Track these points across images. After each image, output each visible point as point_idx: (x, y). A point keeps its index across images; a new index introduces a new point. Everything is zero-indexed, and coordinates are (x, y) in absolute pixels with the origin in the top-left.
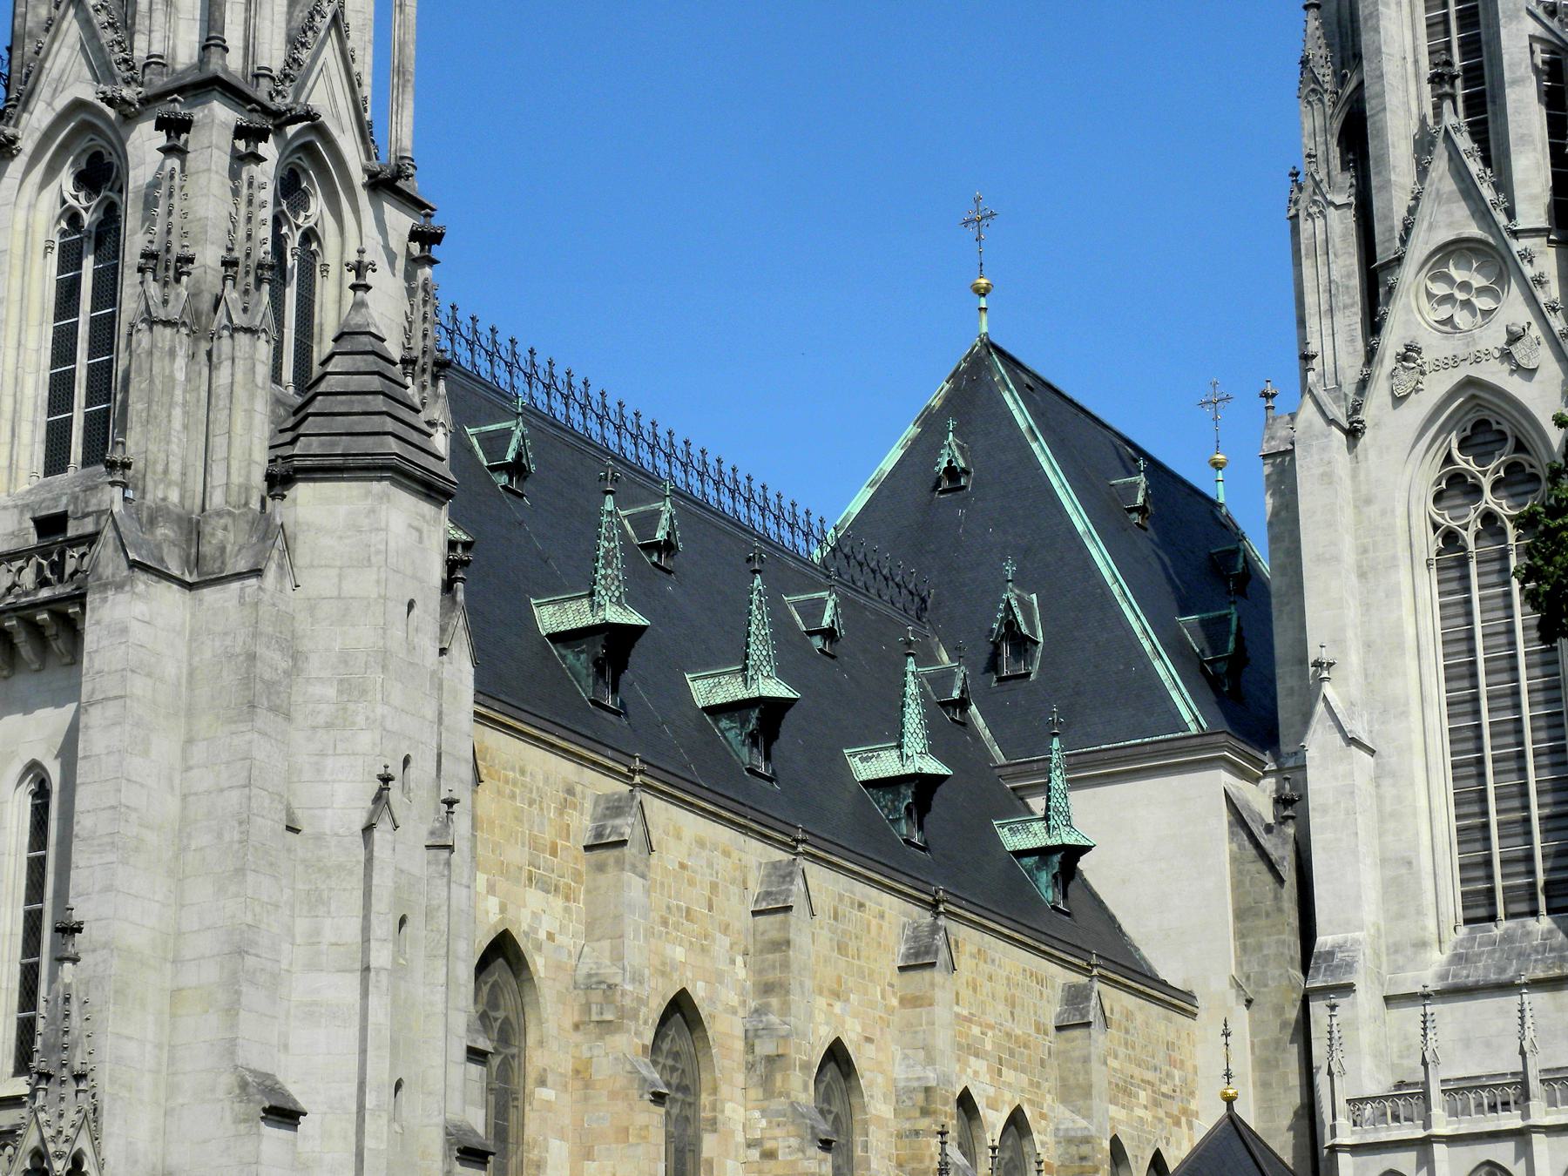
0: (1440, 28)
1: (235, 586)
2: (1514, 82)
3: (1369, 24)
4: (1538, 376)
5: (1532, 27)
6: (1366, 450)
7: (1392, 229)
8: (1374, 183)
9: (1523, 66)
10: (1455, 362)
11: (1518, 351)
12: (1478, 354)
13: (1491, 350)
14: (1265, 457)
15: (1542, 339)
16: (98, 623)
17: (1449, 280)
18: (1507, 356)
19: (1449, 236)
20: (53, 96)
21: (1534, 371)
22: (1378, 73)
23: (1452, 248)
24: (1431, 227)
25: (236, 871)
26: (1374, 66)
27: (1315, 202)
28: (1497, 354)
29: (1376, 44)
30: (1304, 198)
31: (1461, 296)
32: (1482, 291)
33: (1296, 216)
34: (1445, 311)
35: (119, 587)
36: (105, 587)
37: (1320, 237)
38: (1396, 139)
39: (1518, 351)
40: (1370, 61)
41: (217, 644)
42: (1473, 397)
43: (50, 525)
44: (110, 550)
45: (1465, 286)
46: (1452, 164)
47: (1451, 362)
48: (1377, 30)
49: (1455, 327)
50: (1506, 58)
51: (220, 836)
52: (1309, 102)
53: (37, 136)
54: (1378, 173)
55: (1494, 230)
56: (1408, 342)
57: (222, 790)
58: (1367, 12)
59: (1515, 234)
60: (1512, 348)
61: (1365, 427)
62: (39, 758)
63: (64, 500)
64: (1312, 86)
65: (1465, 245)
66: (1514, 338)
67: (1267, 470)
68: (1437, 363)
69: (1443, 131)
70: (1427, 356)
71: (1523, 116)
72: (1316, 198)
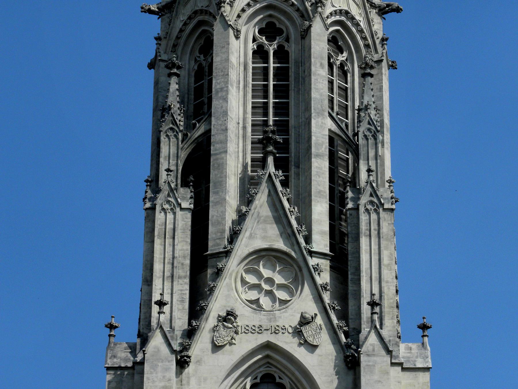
0: (260, 111)
2: (318, 156)
3: (220, 95)
4: (318, 351)
5: (330, 124)
6: (189, 378)
7: (224, 231)
8: (211, 199)
9: (324, 146)
10: (260, 330)
11: (307, 331)
12: (277, 328)
13: (287, 326)
14: (108, 369)
15: (323, 327)
17: (259, 275)
19: (265, 245)
21: (316, 347)
22: (223, 127)
23: (263, 253)
24: (251, 237)
26: (220, 122)
27: (168, 202)
28: (290, 330)
29: (224, 108)
30: (161, 199)
31: (266, 287)
32: (281, 287)
33: (153, 208)
34: (253, 295)
37: (170, 226)
38: (230, 173)
39: (307, 331)
40: (218, 119)
42: (268, 356)
45: (270, 281)
46: (270, 198)
47: (257, 330)
48: (226, 100)
49: (260, 306)
50: (313, 138)
52: (167, 136)
54: (217, 193)
55: (296, 247)
56: (229, 309)
58: (218, 87)
59: (312, 253)
60: (303, 328)
61: (190, 362)
64: (171, 126)
65: (279, 255)
66: (305, 321)
67: (109, 377)
68: (247, 328)
69: (267, 175)
70: (240, 322)
71: (321, 178)
72: (170, 199)
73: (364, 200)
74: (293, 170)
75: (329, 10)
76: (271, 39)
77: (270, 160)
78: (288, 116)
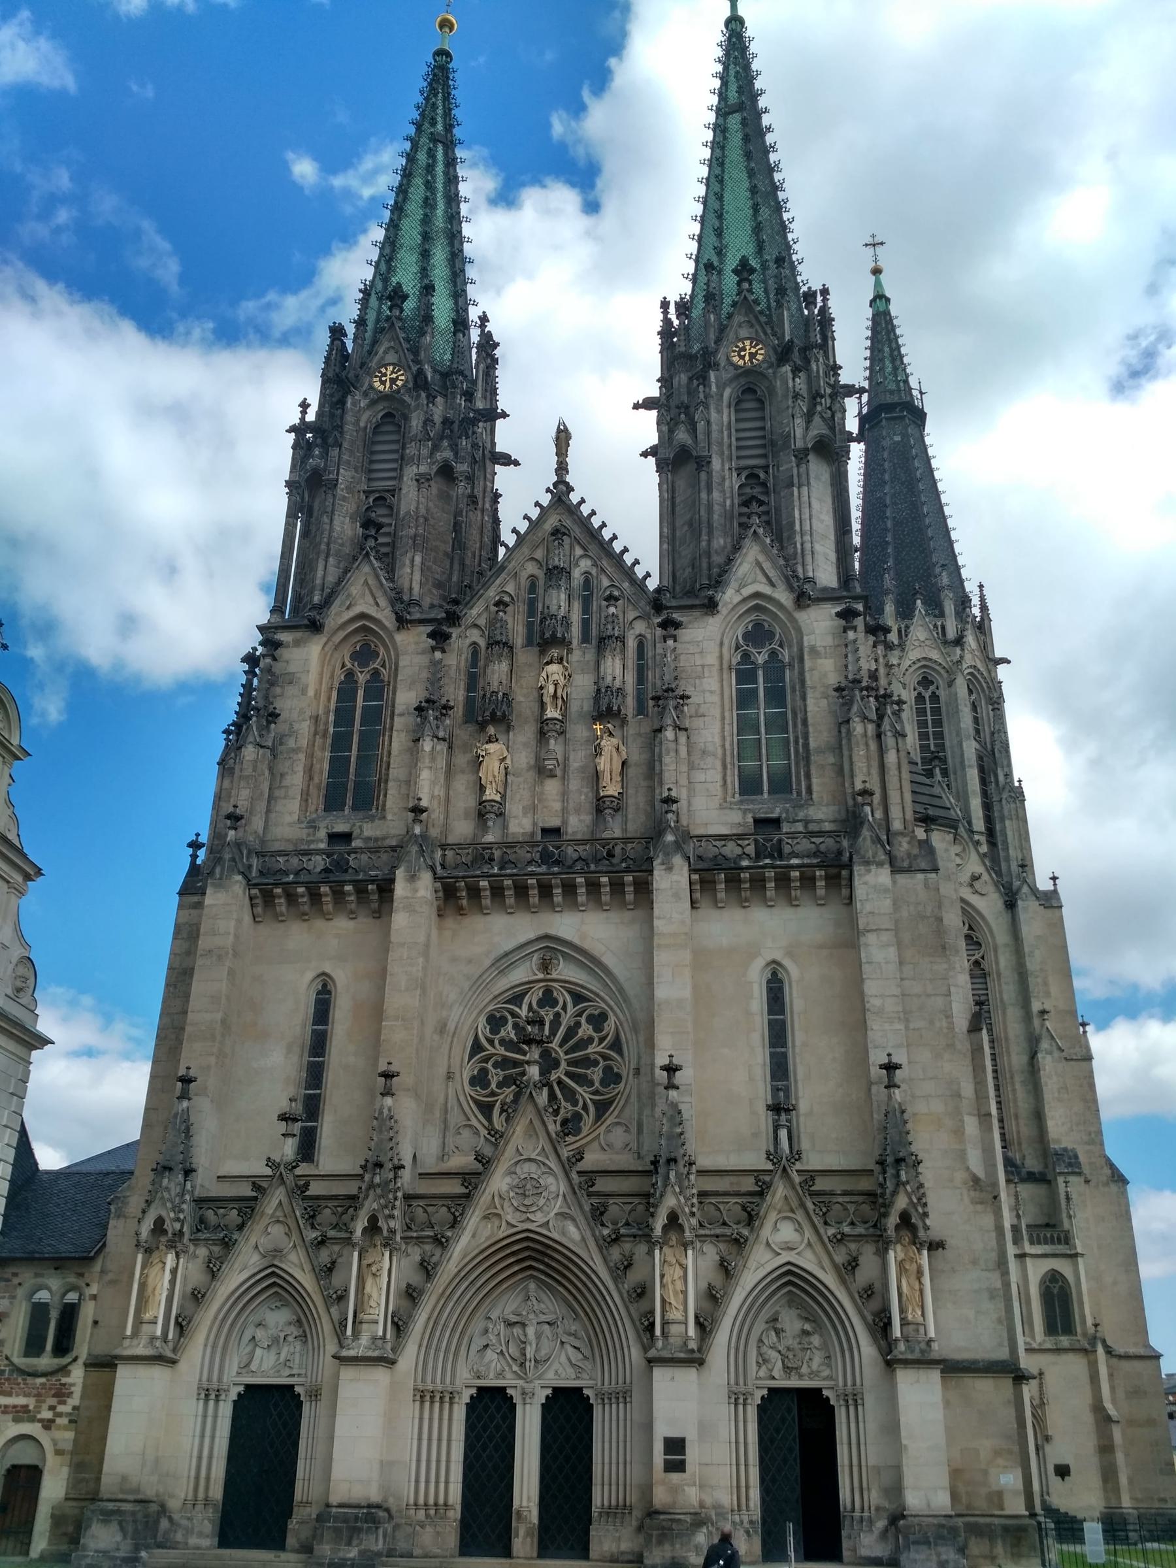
1: (920, 876)
2: (970, 766)
5: (974, 744)
11: (977, 885)
16: (865, 883)
18: (972, 886)
20: (742, 586)
25: (948, 1045)
35: (880, 864)
36: (867, 863)
41: (912, 908)
43: (761, 823)
44: (869, 842)
51: (932, 1022)
53: (730, 606)
57: (929, 996)
62: (778, 956)
63: (778, 810)
73: (1005, 795)
74: (952, 776)
75: (965, 666)
76: (926, 688)
77: (937, 771)
78: (943, 739)
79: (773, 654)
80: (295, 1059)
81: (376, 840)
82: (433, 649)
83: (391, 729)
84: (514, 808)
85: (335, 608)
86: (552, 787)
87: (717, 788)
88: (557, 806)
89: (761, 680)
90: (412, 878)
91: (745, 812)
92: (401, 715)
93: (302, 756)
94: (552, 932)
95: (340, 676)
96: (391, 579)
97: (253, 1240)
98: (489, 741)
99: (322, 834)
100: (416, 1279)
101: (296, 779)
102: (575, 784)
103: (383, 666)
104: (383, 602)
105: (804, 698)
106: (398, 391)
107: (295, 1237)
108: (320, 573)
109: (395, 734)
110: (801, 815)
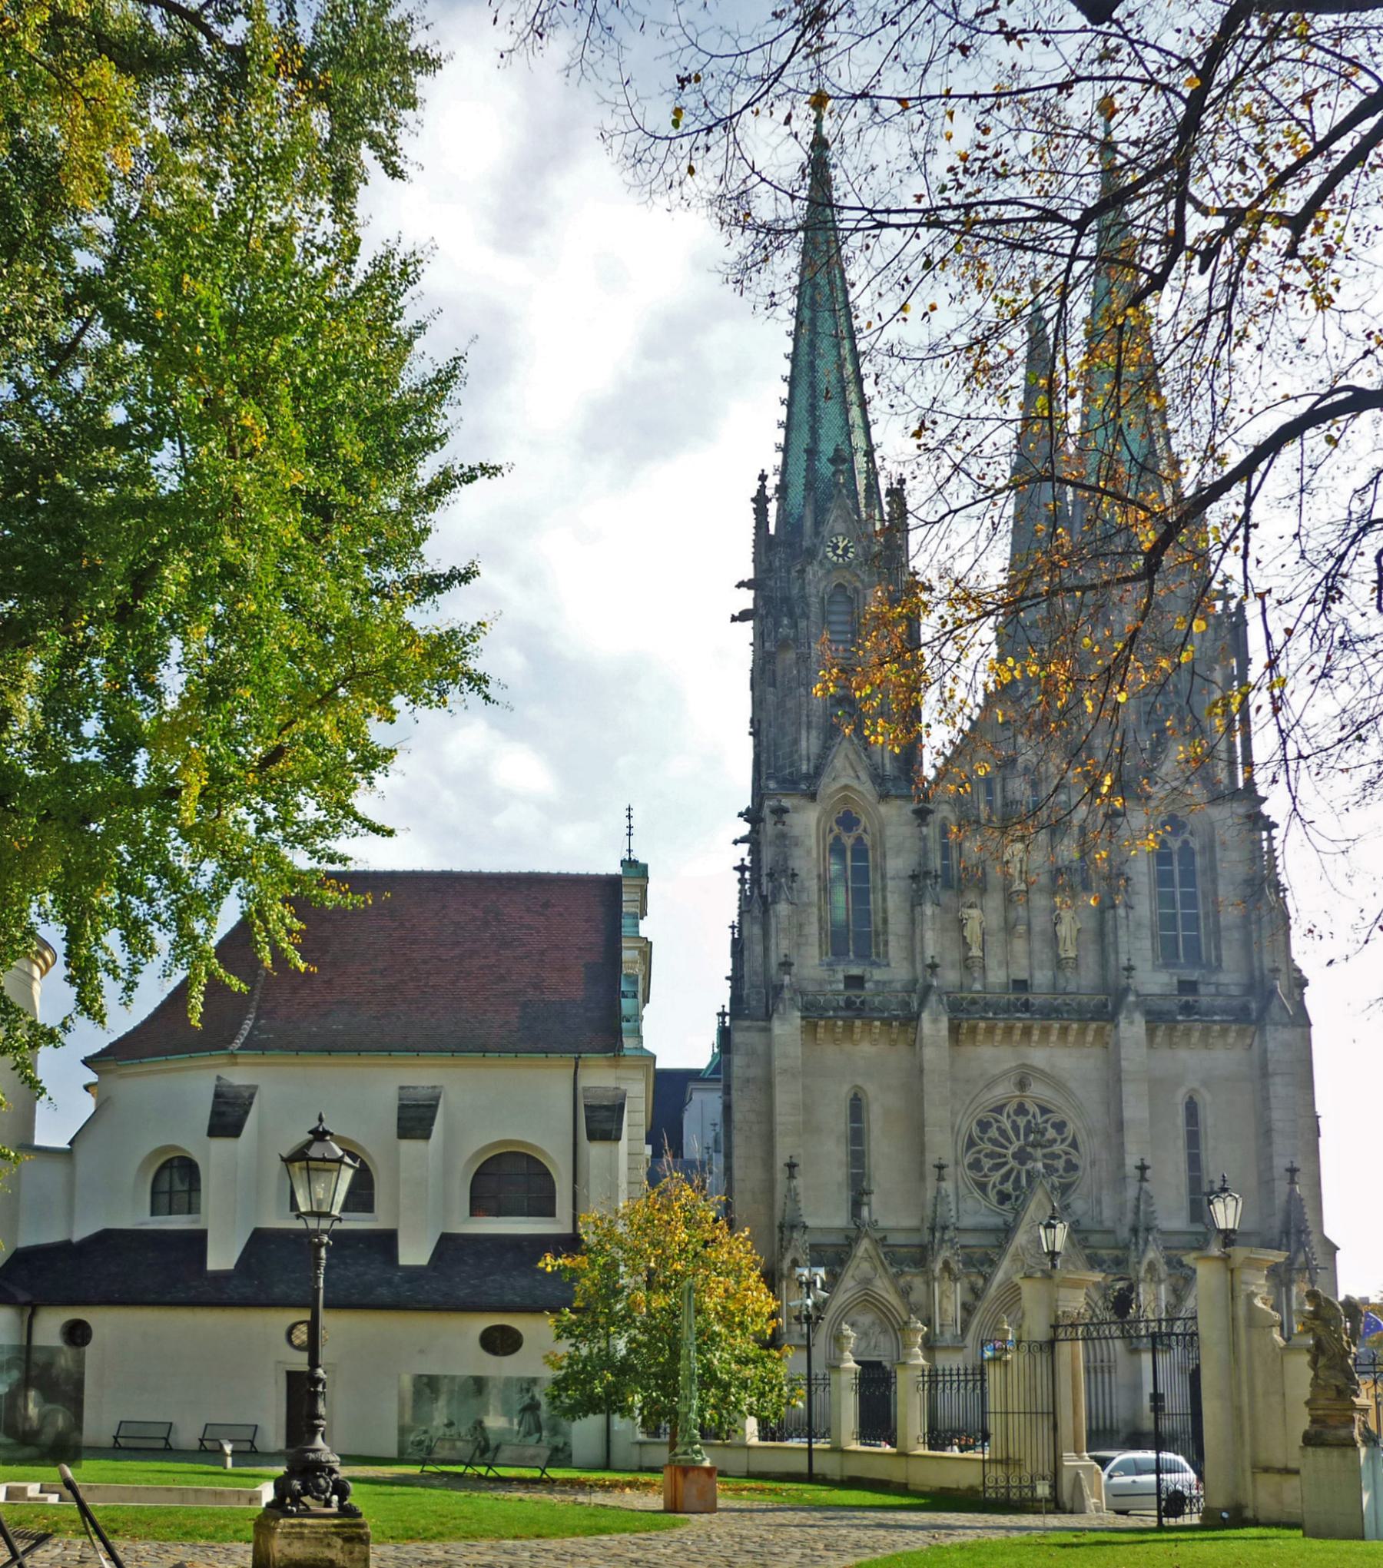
79: (1185, 843)
80: (843, 1148)
81: (884, 983)
82: (919, 826)
83: (884, 888)
84: (992, 963)
85: (824, 780)
86: (1019, 946)
87: (1149, 954)
88: (1024, 962)
89: (1176, 863)
90: (935, 1021)
91: (1172, 975)
92: (893, 878)
93: (815, 910)
94: (1028, 1062)
95: (830, 839)
96: (869, 757)
97: (850, 1273)
98: (970, 907)
99: (840, 976)
100: (970, 1298)
101: (813, 929)
102: (1037, 945)
103: (865, 831)
104: (864, 776)
105: (1214, 881)
106: (850, 564)
107: (880, 1270)
108: (804, 744)
109: (889, 895)
110: (1214, 979)
